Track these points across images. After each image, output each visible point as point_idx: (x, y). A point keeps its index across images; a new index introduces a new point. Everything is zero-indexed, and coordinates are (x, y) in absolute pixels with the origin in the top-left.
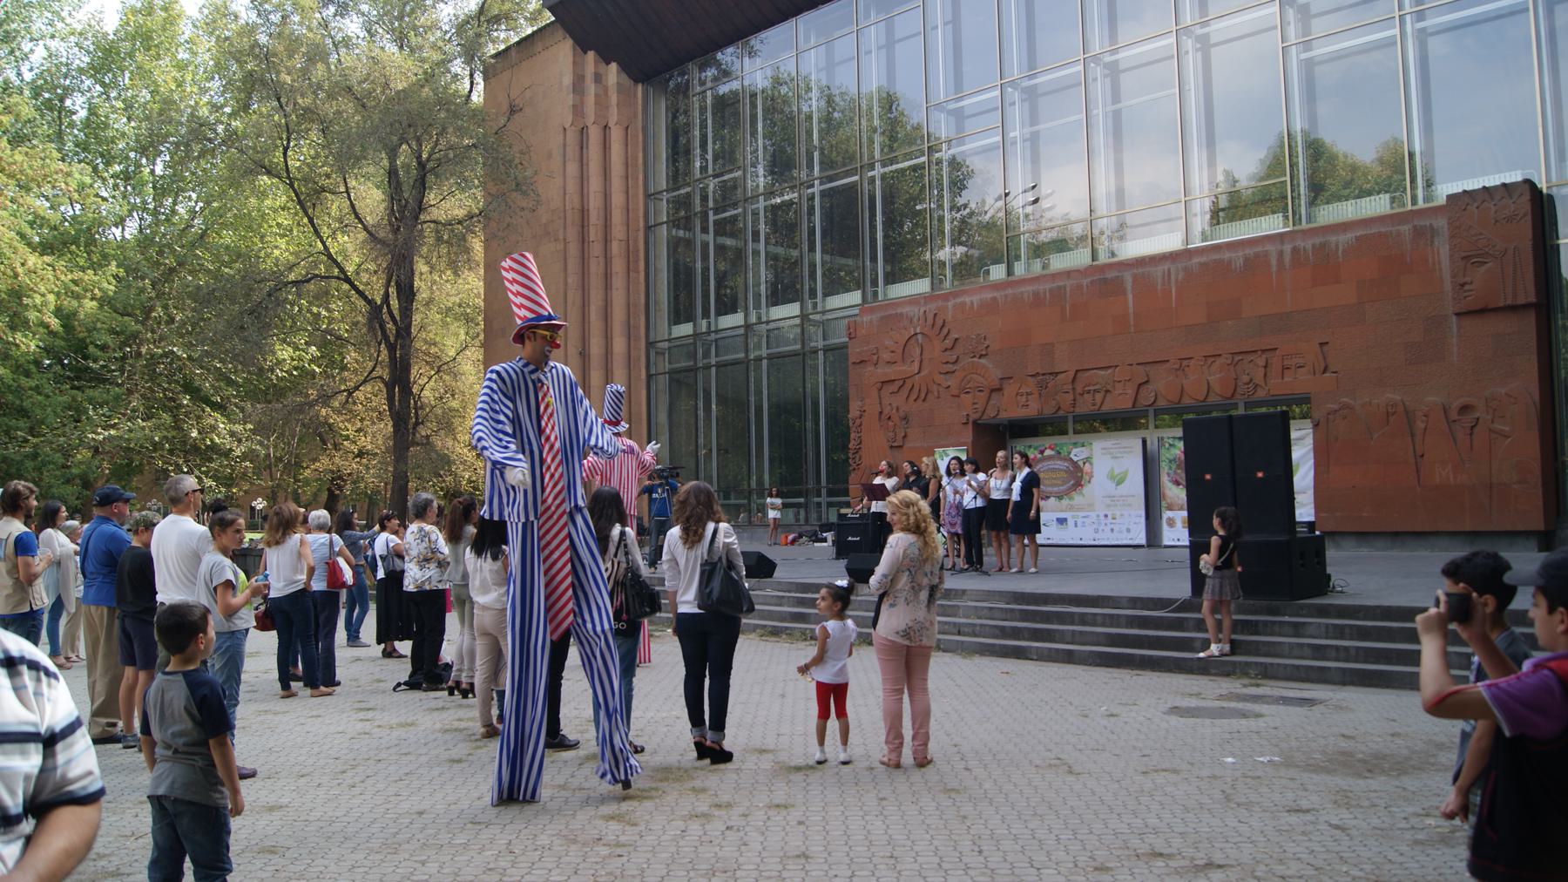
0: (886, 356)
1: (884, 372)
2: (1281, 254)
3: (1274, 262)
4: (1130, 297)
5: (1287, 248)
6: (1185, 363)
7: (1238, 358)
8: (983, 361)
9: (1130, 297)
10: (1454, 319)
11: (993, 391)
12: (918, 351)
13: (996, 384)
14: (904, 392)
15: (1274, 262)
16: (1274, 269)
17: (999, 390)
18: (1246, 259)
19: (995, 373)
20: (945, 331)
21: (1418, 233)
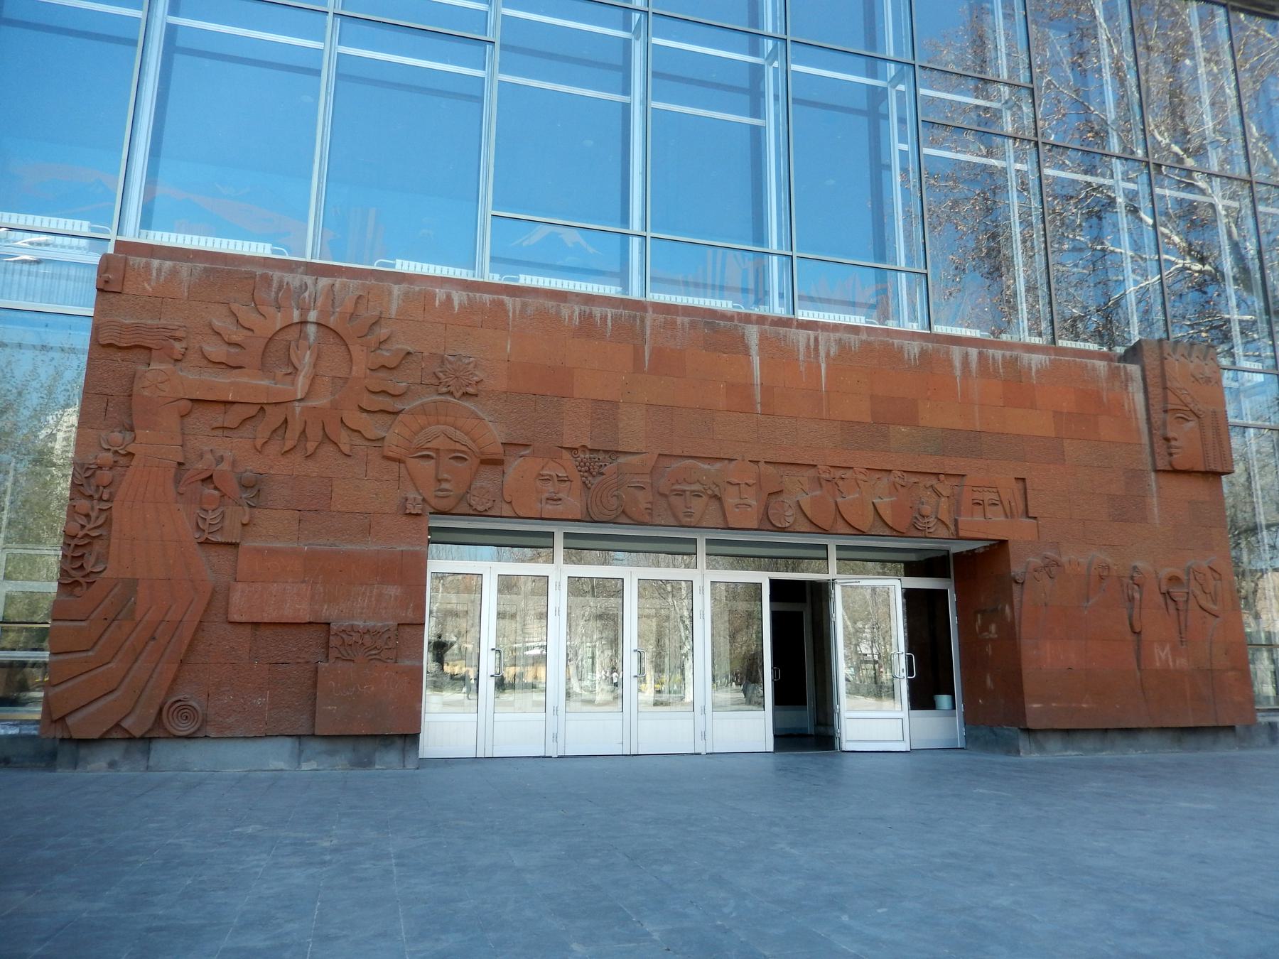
0: (215, 350)
1: (195, 380)
2: (966, 357)
3: (957, 363)
4: (756, 360)
5: (973, 352)
6: (839, 473)
7: (914, 479)
8: (469, 404)
9: (756, 360)
10: (1153, 475)
11: (484, 462)
12: (308, 357)
13: (496, 450)
14: (263, 430)
15: (957, 363)
16: (958, 372)
17: (496, 462)
18: (923, 353)
19: (494, 434)
20: (383, 332)
21: (1114, 374)
